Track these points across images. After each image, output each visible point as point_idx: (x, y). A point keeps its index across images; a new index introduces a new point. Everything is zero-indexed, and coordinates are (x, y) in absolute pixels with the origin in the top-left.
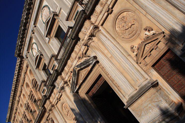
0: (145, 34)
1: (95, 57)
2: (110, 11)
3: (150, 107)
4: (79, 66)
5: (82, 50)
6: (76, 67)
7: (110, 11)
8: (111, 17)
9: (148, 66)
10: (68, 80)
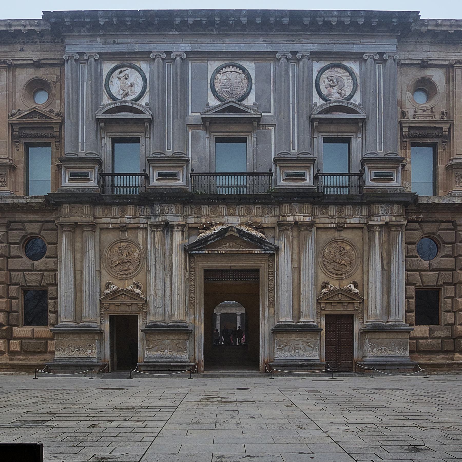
0: (350, 286)
1: (277, 249)
2: (341, 229)
3: (300, 348)
4: (242, 233)
5: (263, 220)
6: (235, 230)
7: (341, 229)
8: (336, 234)
9: (323, 312)
10: (190, 226)
